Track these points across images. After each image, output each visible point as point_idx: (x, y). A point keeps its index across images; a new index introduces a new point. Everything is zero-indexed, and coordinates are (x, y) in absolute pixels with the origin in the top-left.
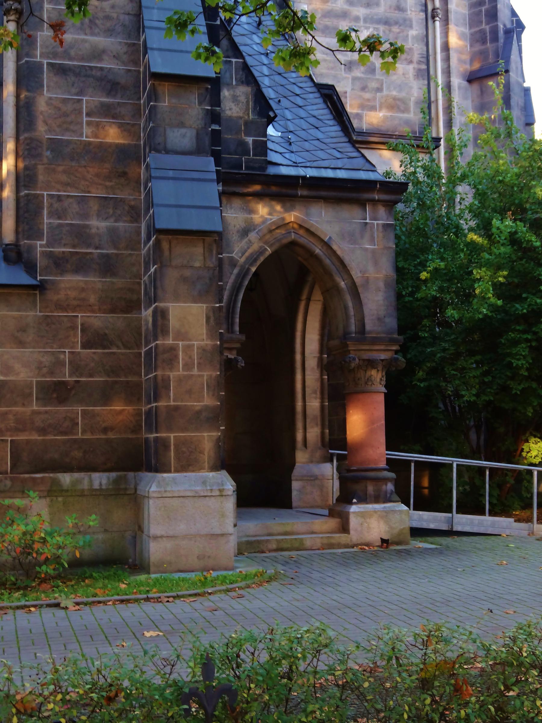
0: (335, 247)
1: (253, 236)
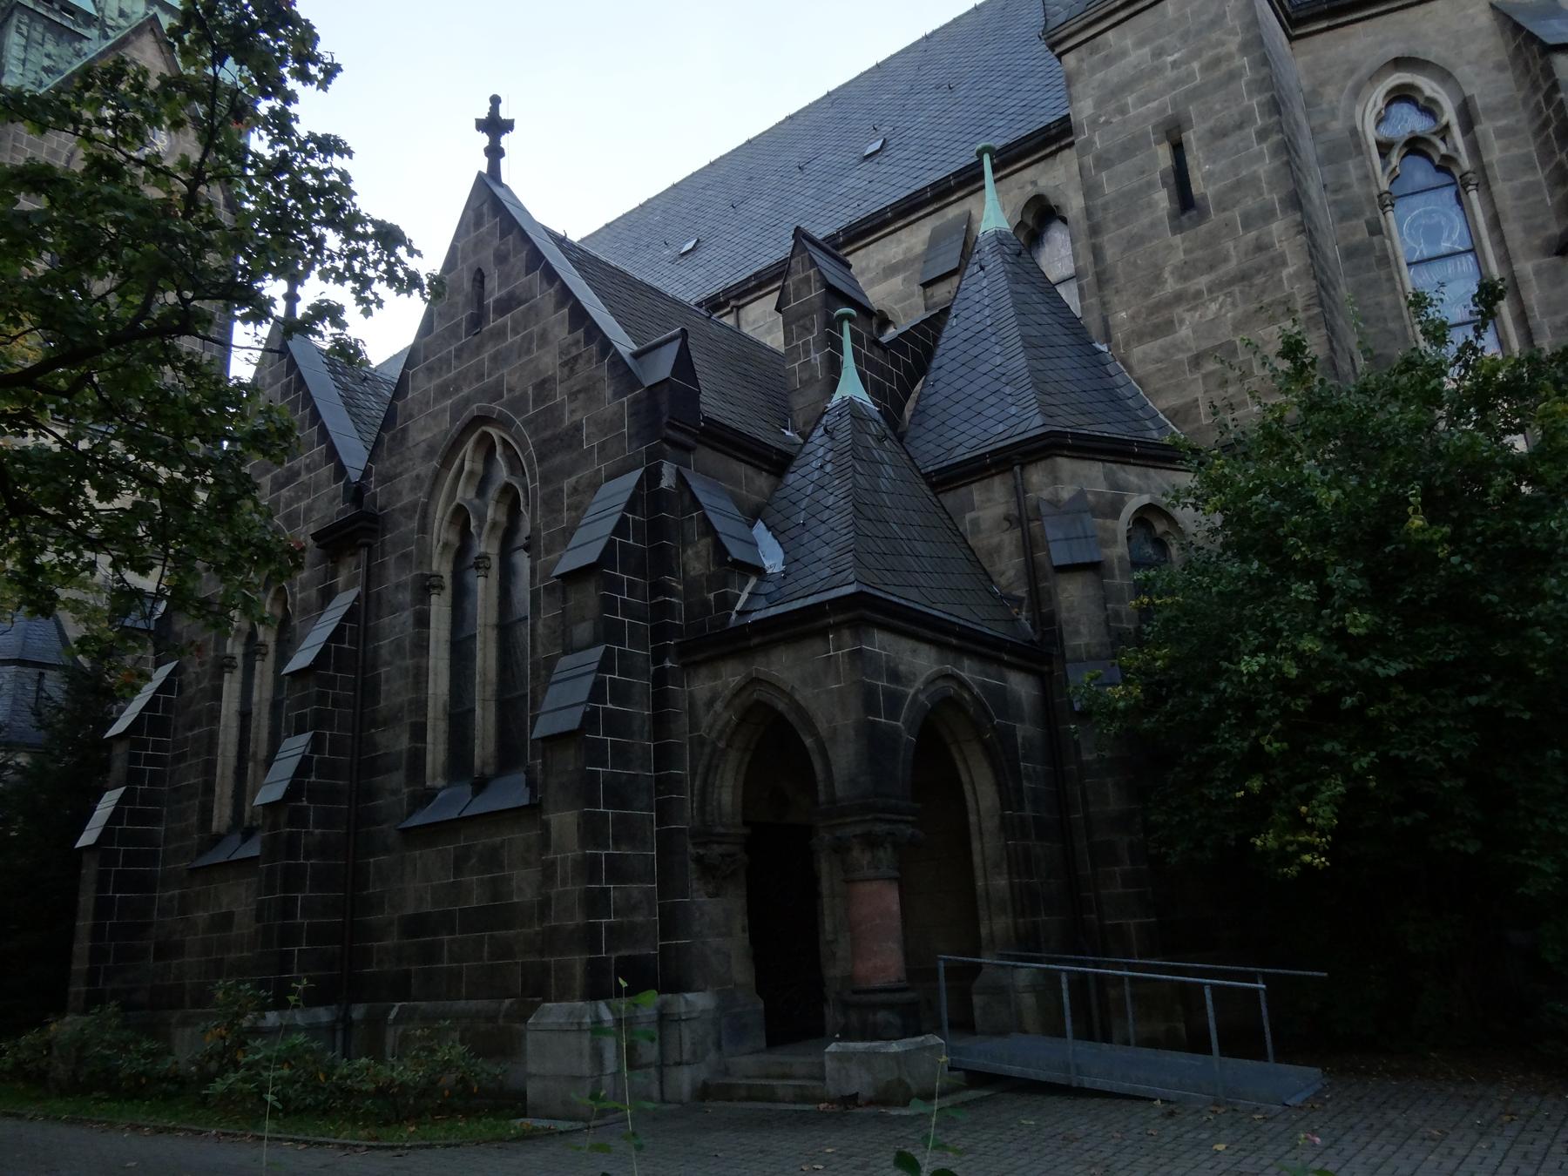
0: (797, 697)
1: (719, 706)
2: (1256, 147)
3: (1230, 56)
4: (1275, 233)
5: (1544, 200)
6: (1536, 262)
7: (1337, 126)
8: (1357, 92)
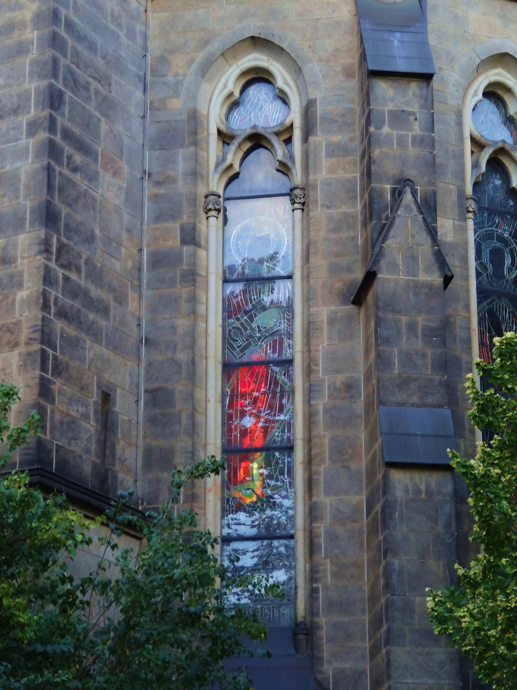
2: (23, 141)
3: (22, 26)
4: (20, 248)
5: (354, 238)
6: (333, 308)
7: (176, 104)
8: (206, 69)
